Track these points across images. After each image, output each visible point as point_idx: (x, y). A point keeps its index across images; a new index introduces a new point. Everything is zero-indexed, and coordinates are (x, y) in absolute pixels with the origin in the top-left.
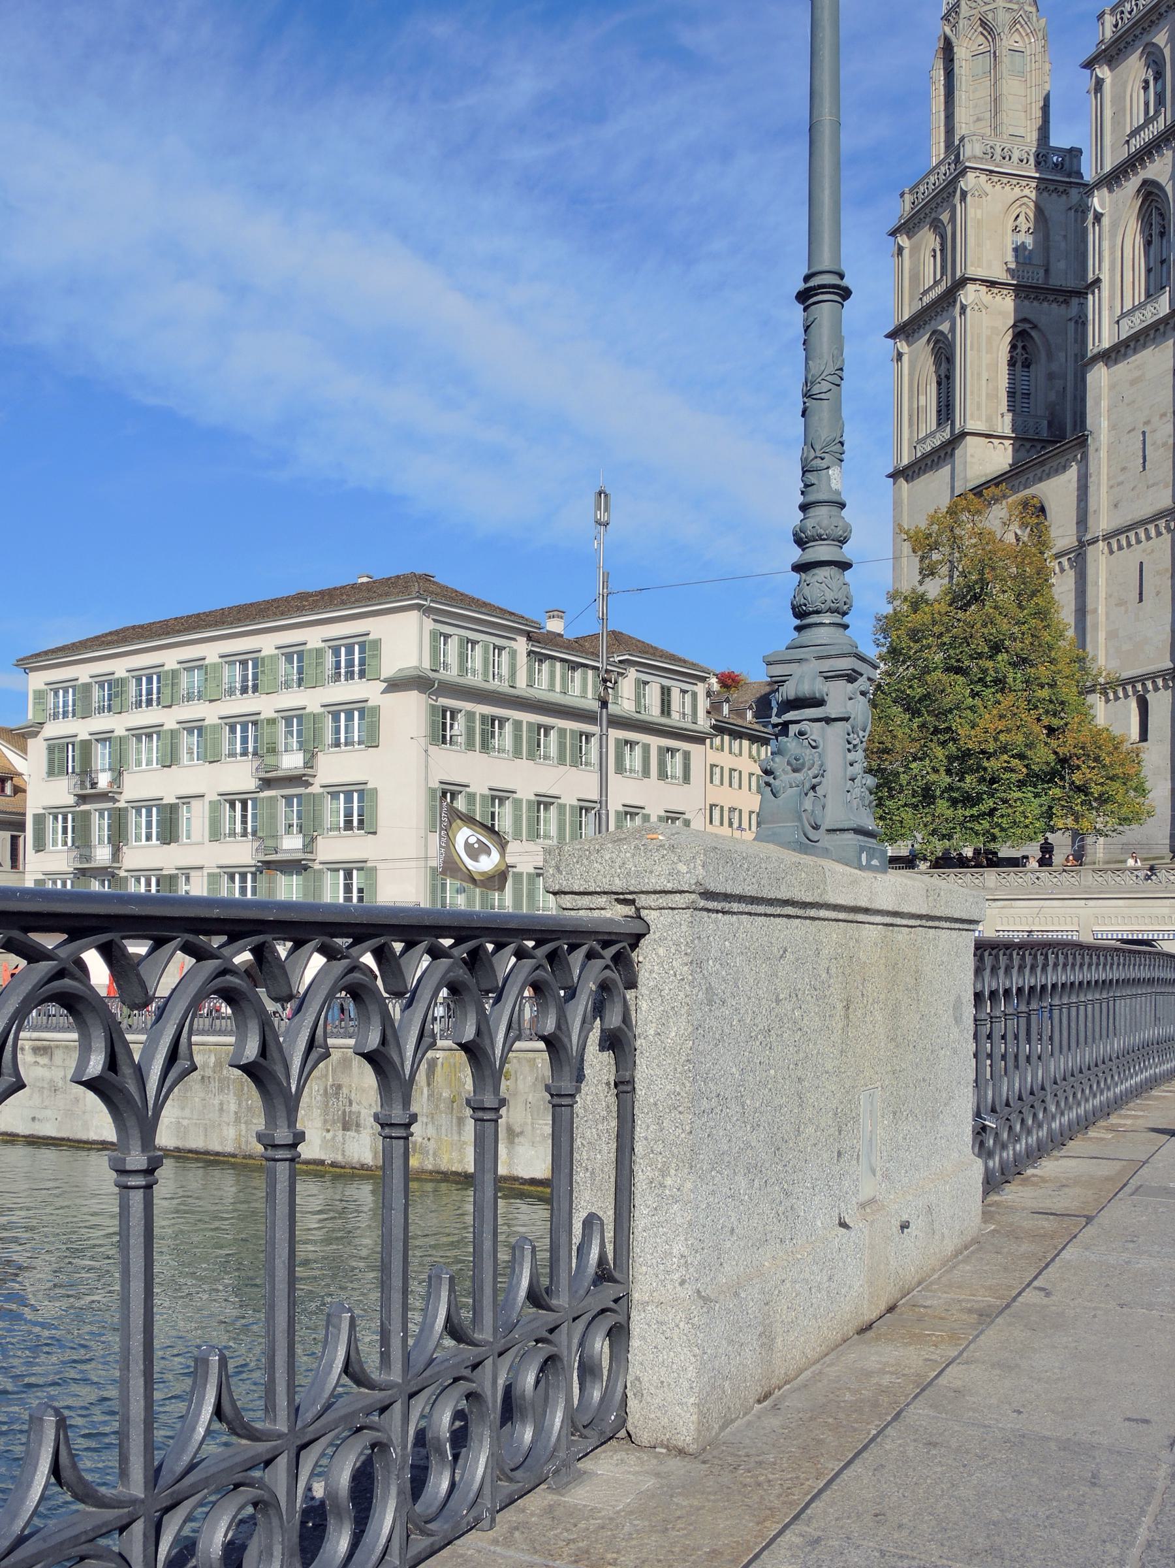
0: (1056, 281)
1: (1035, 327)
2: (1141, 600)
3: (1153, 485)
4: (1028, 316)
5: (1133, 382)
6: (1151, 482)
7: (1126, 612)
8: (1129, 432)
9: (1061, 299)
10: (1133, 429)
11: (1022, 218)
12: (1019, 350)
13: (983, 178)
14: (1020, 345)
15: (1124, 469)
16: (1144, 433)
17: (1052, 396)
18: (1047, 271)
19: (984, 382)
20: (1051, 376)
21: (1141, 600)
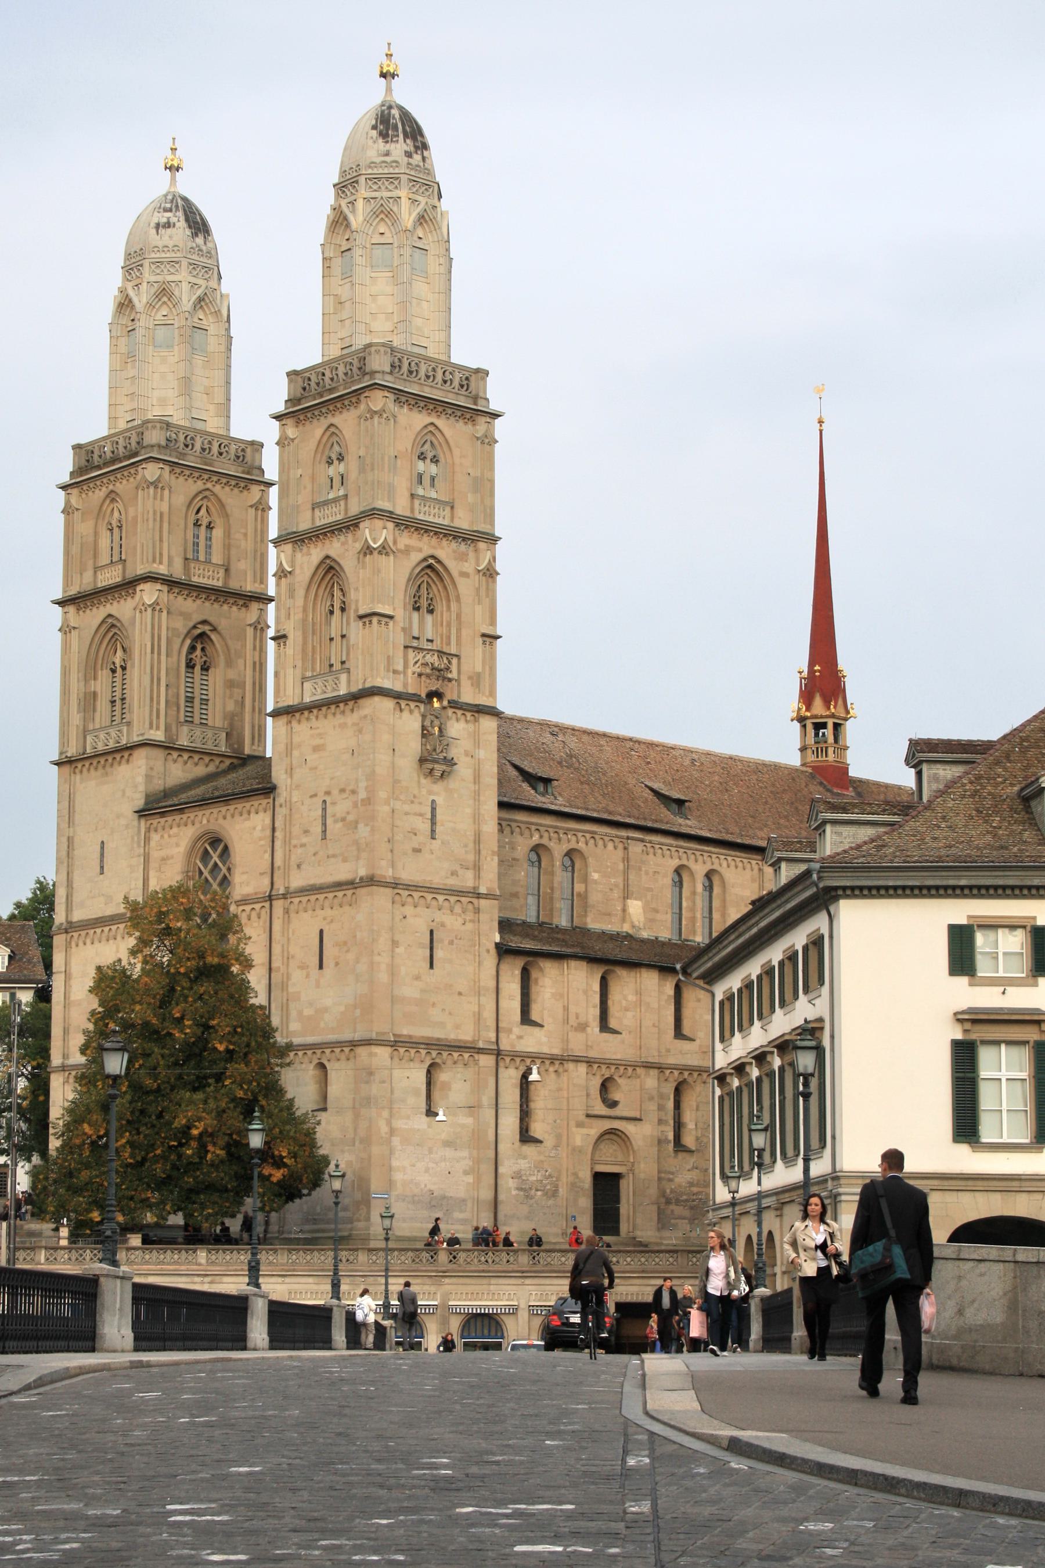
0: (234, 585)
1: (214, 629)
2: (321, 967)
3: (334, 856)
4: (211, 619)
5: (316, 749)
6: (330, 853)
7: (308, 976)
8: (311, 797)
9: (241, 602)
10: (315, 795)
11: (203, 511)
12: (198, 652)
13: (167, 468)
14: (199, 646)
15: (306, 832)
16: (324, 802)
17: (231, 707)
18: (227, 570)
19: (163, 689)
20: (230, 684)
21: (321, 967)
